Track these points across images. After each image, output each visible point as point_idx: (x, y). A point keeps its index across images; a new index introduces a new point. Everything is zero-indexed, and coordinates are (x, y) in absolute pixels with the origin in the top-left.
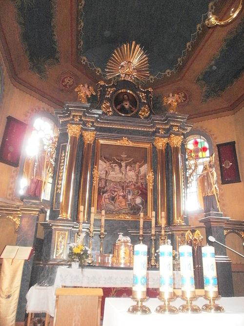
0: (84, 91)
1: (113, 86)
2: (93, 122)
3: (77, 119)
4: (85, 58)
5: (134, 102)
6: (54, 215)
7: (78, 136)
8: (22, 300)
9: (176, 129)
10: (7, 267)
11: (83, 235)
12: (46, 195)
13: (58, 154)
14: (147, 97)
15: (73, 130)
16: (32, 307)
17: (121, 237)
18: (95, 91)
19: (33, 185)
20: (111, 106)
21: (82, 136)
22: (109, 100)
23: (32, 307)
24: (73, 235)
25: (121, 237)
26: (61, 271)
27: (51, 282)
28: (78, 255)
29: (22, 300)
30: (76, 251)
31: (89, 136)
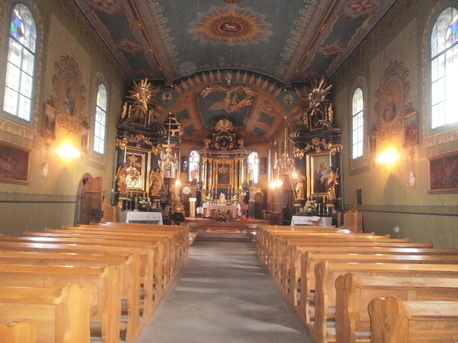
0: (207, 142)
1: (219, 135)
2: (211, 154)
3: (205, 154)
4: (206, 126)
5: (228, 142)
6: (201, 188)
7: (206, 161)
8: (196, 211)
9: (242, 154)
10: (191, 204)
11: (210, 194)
12: (198, 181)
13: (200, 166)
14: (233, 139)
15: (204, 160)
16: (198, 212)
17: (222, 194)
18: (212, 140)
19: (194, 181)
20: (218, 145)
21: (208, 161)
22: (217, 142)
23: (198, 212)
24: (207, 195)
25: (222, 194)
26: (204, 204)
27: (202, 207)
28: (209, 200)
29: (196, 211)
30: (208, 199)
31: (210, 161)
